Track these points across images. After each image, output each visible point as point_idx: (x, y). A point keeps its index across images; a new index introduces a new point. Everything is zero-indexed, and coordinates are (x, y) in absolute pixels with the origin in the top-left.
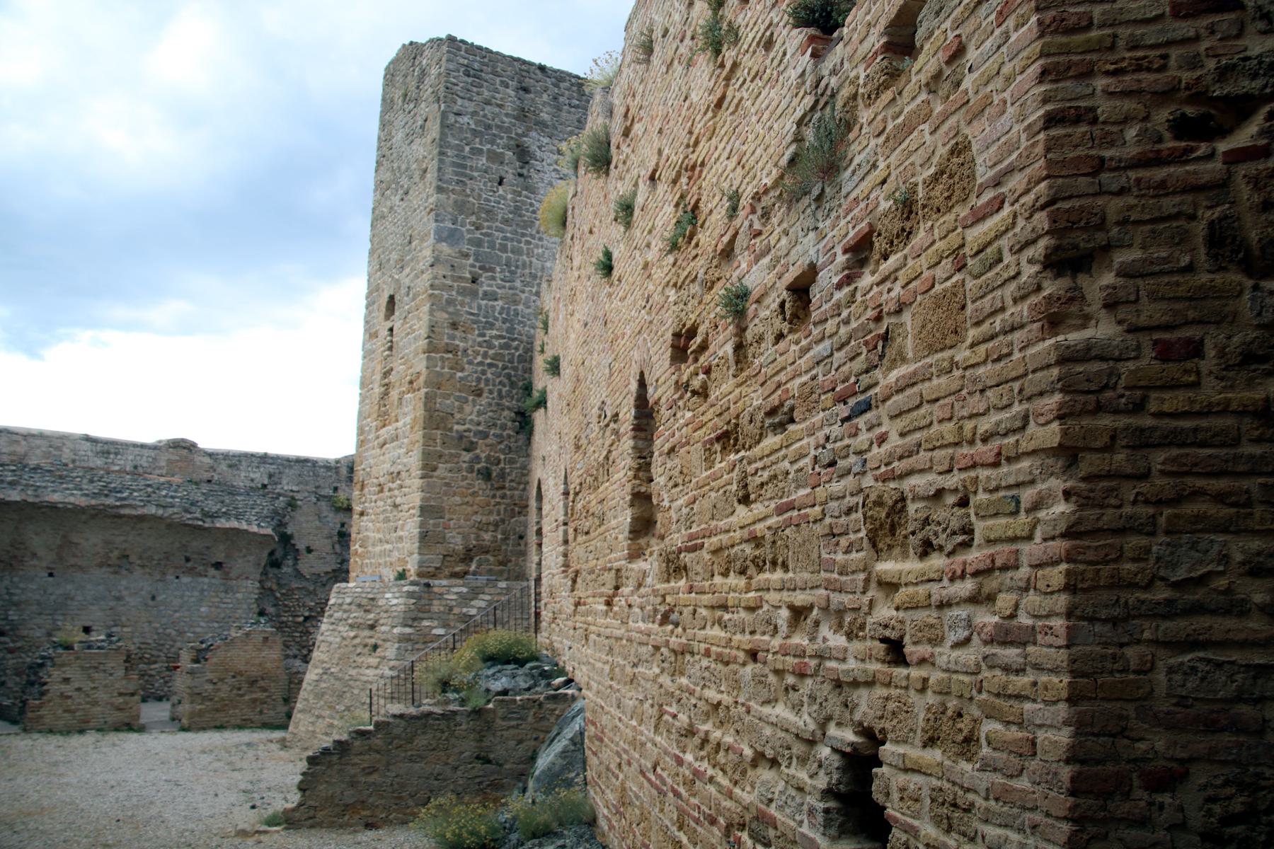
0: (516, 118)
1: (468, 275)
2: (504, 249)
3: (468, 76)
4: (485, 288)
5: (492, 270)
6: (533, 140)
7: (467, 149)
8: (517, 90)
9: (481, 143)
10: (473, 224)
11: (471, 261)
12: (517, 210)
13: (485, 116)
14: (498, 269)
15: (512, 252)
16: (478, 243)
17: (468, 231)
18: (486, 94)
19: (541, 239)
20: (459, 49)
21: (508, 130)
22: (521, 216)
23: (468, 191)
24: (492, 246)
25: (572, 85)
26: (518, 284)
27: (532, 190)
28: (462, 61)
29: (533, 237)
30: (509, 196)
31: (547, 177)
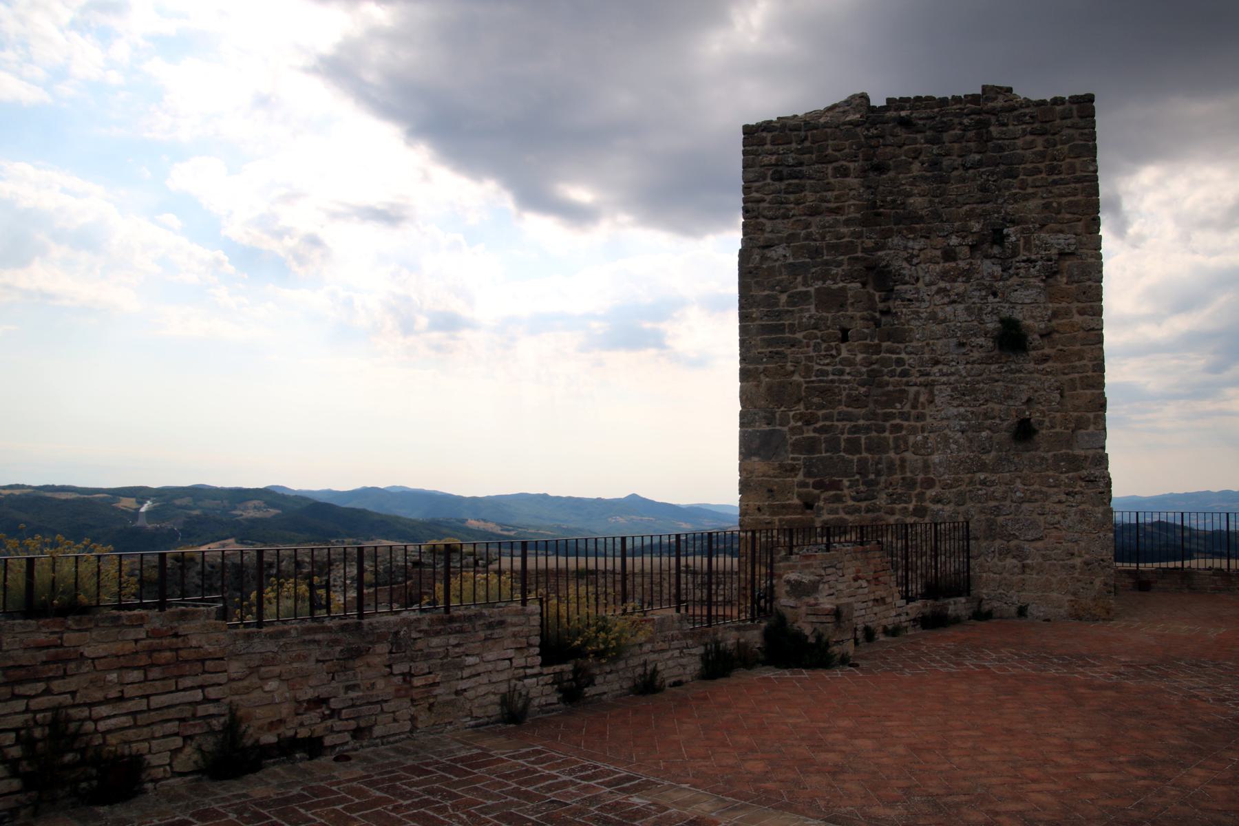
0: (864, 222)
1: (796, 501)
2: (853, 446)
3: (781, 179)
4: (826, 517)
5: (836, 486)
6: (894, 254)
7: (784, 298)
8: (863, 173)
9: (805, 284)
10: (800, 417)
11: (800, 477)
12: (873, 378)
13: (808, 237)
14: (846, 482)
15: (868, 450)
16: (810, 446)
17: (792, 429)
18: (810, 198)
19: (921, 417)
20: (762, 142)
21: (849, 248)
22: (882, 385)
23: (789, 367)
24: (833, 445)
25: (966, 129)
26: (882, 500)
27: (898, 336)
28: (766, 160)
29: (905, 416)
30: (860, 357)
31: (924, 309)
